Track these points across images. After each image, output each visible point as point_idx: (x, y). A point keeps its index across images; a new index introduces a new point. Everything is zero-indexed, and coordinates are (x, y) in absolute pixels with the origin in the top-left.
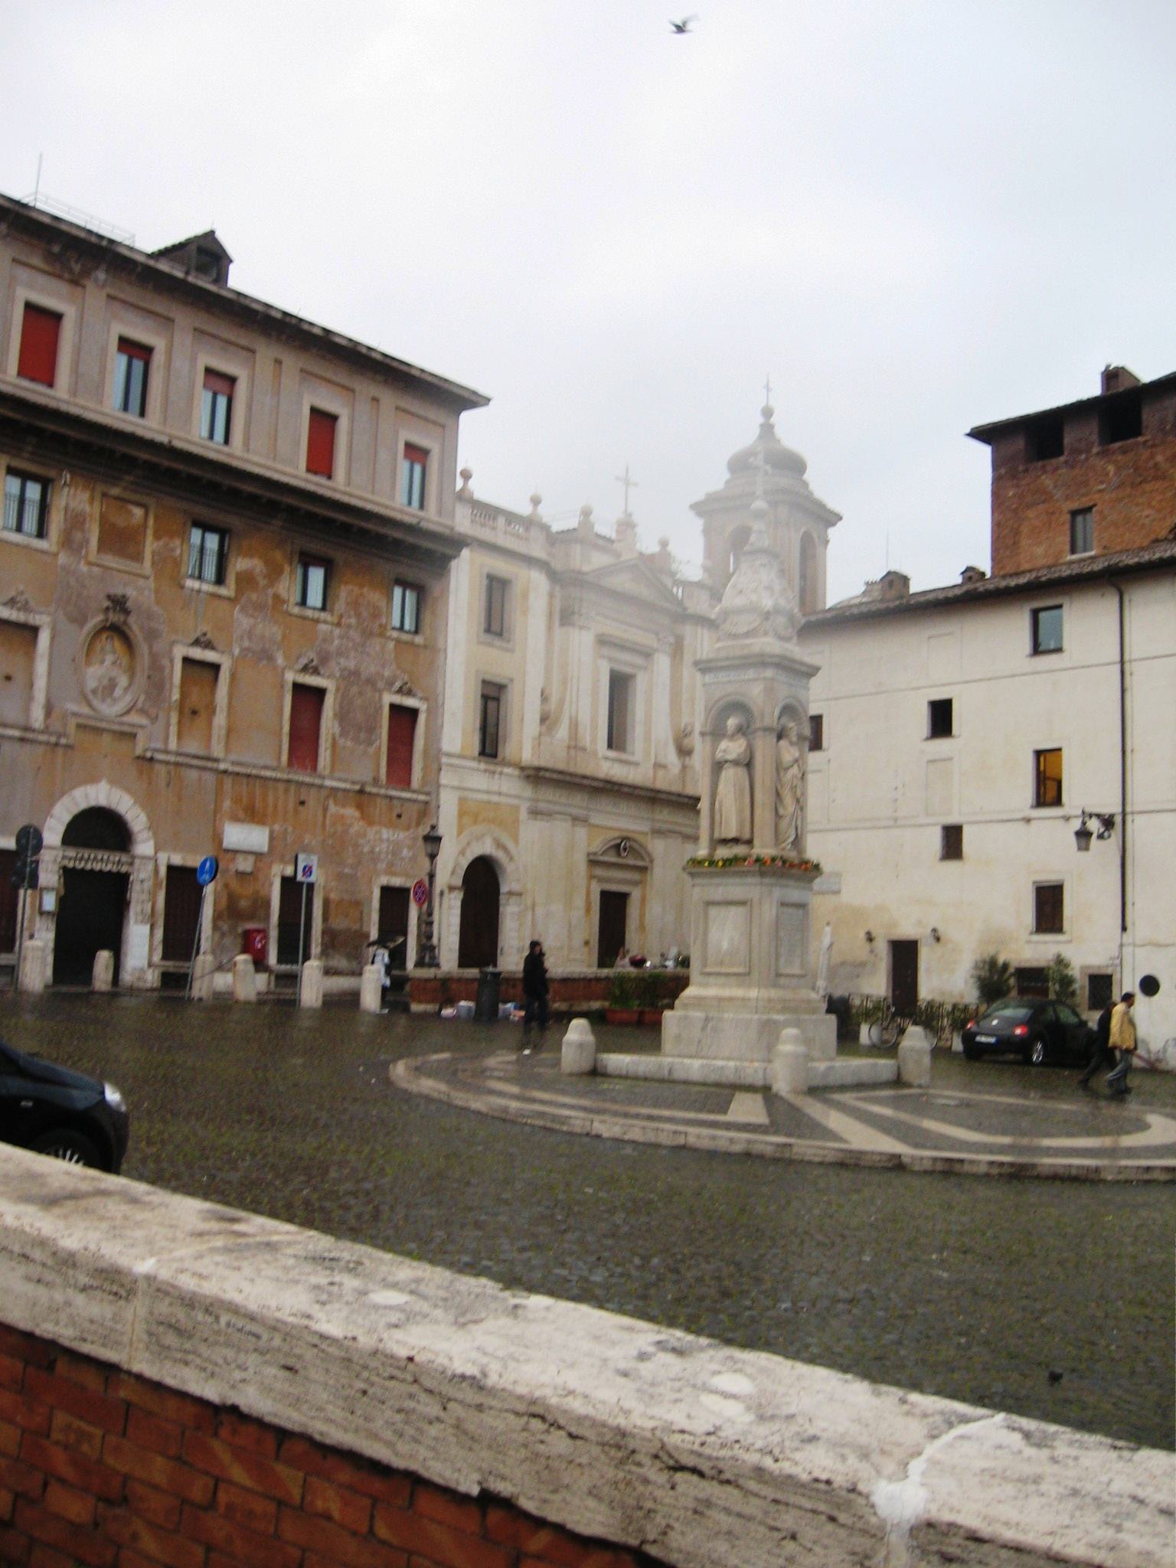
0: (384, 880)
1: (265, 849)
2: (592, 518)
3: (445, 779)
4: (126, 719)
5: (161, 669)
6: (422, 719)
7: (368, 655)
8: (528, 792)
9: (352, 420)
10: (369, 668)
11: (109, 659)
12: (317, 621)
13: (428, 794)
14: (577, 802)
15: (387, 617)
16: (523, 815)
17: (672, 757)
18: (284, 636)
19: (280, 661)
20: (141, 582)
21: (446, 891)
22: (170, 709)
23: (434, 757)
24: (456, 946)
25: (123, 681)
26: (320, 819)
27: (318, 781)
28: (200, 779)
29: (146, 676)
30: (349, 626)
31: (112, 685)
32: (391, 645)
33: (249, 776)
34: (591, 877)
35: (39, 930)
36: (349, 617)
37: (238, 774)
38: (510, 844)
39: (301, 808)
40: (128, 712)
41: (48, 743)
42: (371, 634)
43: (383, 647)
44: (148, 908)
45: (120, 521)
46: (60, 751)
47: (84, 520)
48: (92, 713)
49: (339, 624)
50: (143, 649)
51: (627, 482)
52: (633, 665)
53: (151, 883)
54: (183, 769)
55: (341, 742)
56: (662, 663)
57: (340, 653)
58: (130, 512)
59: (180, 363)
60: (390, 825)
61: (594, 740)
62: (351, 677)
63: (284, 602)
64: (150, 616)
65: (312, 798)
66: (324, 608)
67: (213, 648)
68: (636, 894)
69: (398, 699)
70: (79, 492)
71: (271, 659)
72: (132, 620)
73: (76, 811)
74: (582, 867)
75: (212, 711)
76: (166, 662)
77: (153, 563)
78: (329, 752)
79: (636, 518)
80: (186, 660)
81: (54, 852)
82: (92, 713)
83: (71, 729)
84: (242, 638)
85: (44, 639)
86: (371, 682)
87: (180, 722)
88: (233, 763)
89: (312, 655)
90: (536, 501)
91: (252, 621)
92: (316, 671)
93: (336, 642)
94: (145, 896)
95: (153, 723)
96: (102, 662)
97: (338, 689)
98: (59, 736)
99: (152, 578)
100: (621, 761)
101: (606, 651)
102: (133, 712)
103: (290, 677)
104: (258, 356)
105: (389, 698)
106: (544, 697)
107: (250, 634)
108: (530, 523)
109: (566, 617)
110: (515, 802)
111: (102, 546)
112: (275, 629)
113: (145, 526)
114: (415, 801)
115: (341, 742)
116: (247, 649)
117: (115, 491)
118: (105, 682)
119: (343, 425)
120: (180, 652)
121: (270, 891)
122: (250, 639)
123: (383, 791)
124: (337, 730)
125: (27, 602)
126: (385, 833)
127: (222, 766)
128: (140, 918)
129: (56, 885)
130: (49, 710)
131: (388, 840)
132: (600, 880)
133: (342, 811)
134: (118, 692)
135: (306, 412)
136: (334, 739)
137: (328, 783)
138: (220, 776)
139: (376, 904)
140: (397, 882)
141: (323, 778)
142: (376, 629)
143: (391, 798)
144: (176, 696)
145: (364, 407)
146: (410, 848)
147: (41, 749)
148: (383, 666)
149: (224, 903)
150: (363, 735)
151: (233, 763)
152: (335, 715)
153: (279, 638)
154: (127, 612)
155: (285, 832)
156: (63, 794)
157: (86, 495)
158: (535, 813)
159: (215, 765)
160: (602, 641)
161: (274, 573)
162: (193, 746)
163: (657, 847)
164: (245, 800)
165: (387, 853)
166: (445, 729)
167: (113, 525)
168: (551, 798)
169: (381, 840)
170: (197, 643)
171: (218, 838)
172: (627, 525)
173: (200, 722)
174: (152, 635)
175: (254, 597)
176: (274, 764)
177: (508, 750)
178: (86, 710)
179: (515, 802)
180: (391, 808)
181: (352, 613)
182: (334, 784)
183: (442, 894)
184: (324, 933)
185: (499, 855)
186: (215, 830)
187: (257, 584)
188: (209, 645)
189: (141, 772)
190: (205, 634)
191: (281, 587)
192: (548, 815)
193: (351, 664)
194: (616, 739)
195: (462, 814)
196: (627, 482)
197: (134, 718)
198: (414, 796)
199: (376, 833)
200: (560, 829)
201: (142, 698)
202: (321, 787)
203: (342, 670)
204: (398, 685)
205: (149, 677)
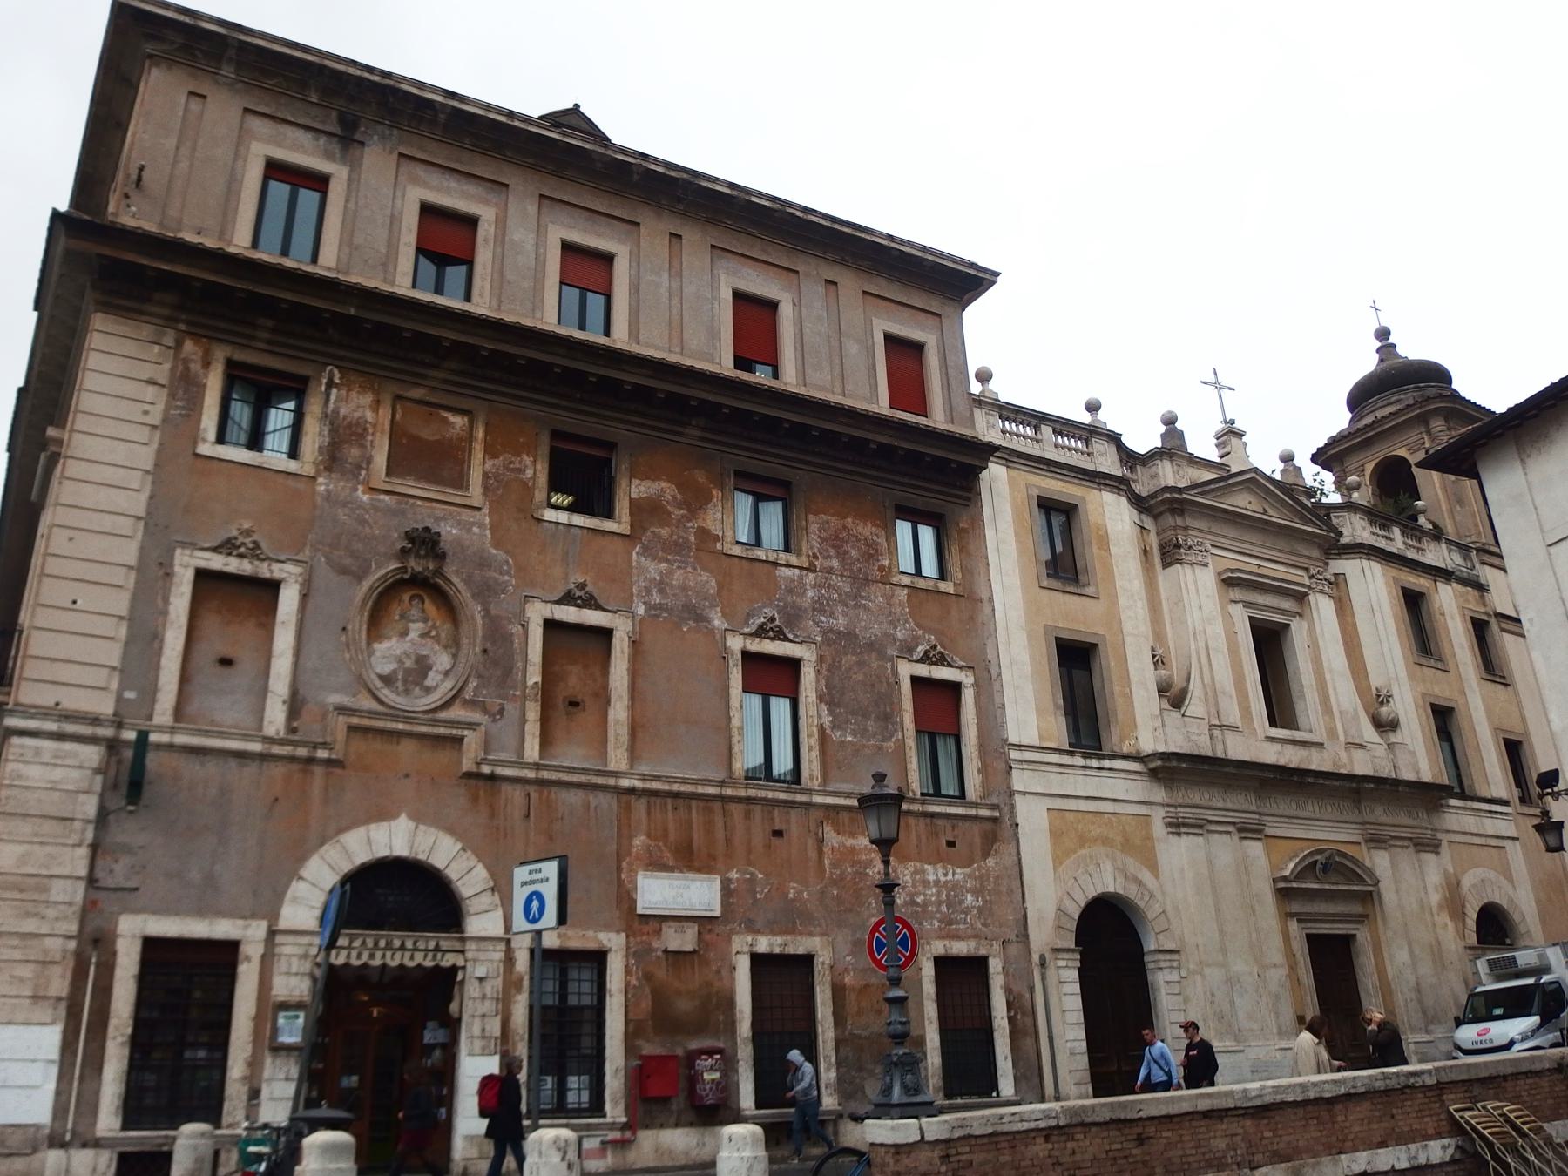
0: (939, 947)
1: (718, 913)
2: (1178, 425)
3: (1020, 780)
4: (443, 715)
5: (507, 638)
6: (968, 696)
7: (867, 609)
8: (1159, 794)
9: (798, 305)
10: (871, 627)
11: (416, 629)
12: (776, 564)
13: (994, 807)
14: (1239, 804)
15: (890, 553)
16: (1159, 829)
17: (1369, 733)
18: (720, 586)
19: (718, 622)
20: (466, 515)
22: (524, 697)
23: (997, 751)
24: (1083, 1046)
25: (443, 661)
26: (813, 854)
27: (804, 798)
28: (587, 806)
29: (477, 650)
30: (830, 571)
31: (423, 666)
32: (903, 594)
33: (677, 795)
35: (270, 1080)
36: (828, 557)
37: (655, 793)
38: (1146, 876)
39: (775, 841)
40: (446, 705)
41: (293, 759)
42: (867, 581)
43: (889, 598)
44: (495, 1027)
45: (428, 433)
46: (319, 771)
47: (365, 429)
48: (375, 706)
49: (811, 569)
50: (474, 611)
51: (1218, 386)
52: (1283, 611)
53: (499, 982)
54: (554, 789)
55: (836, 736)
56: (1323, 607)
57: (819, 608)
58: (445, 420)
59: (522, 235)
60: (937, 859)
61: (1246, 711)
62: (837, 643)
63: (717, 538)
64: (484, 563)
65: (794, 823)
66: (787, 549)
67: (598, 607)
68: (1363, 935)
69: (923, 670)
70: (354, 394)
71: (701, 619)
72: (450, 570)
73: (346, 867)
74: (1269, 897)
75: (603, 697)
76: (515, 629)
77: (487, 489)
78: (815, 753)
79: (1238, 425)
80: (550, 625)
81: (305, 940)
82: (375, 706)
83: (341, 735)
84: (648, 590)
85: (288, 599)
86: (875, 646)
87: (545, 721)
88: (644, 778)
89: (769, 612)
90: (1093, 407)
91: (664, 566)
92: (780, 635)
93: (810, 593)
94: (488, 1007)
95: (494, 721)
96: (404, 633)
97: (821, 659)
98: (315, 746)
99: (486, 511)
100: (1294, 742)
101: (1237, 594)
102: (457, 703)
103: (736, 643)
104: (642, 229)
105: (906, 670)
106: (1159, 662)
107: (662, 586)
108: (1089, 433)
109: (1170, 554)
110: (1142, 810)
111: (394, 467)
112: (705, 576)
113: (471, 438)
114: (976, 818)
115: (836, 736)
116: (659, 607)
117: (417, 393)
118: (409, 664)
119: (786, 312)
120: (537, 613)
121: (733, 980)
122: (661, 591)
124: (827, 720)
125: (257, 545)
126: (932, 873)
127: (625, 783)
128: (478, 1044)
129: (307, 999)
130: (295, 706)
131: (937, 882)
132: (1302, 918)
133: (850, 842)
134: (432, 678)
135: (727, 295)
136: (821, 728)
137: (818, 799)
138: (624, 798)
139: (929, 987)
140: (961, 948)
141: (810, 792)
143: (933, 815)
144: (534, 677)
145: (814, 292)
146: (977, 892)
147: (278, 770)
148: (894, 625)
149: (646, 1004)
150: (871, 725)
151: (644, 778)
152: (820, 698)
153: (712, 589)
154: (441, 557)
155: (753, 880)
156: (323, 841)
157: (368, 399)
158: (1176, 826)
159: (612, 781)
160: (1229, 582)
161: (696, 501)
162: (573, 755)
163: (1380, 862)
164: (672, 837)
165: (940, 903)
166: (1009, 710)
167: (415, 439)
168: (1197, 800)
169: (926, 883)
170: (567, 599)
171: (626, 898)
172: (1230, 434)
173: (587, 717)
174: (486, 592)
175: (665, 532)
176: (720, 776)
177: (1114, 738)
178: (369, 704)
179: (1142, 810)
180: (934, 834)
181: (832, 552)
182: (830, 800)
183: (1043, 965)
184: (838, 1043)
185: (1131, 892)
186: (620, 882)
187: (669, 514)
188: (590, 602)
189: (475, 799)
190: (582, 586)
191: (709, 517)
192: (1198, 827)
193: (840, 623)
194: (1280, 708)
195: (1056, 835)
196: (1218, 386)
197: (457, 713)
198: (973, 812)
199: (916, 872)
200: (1224, 848)
201: (473, 683)
202: (808, 806)
203: (824, 632)
204: (921, 649)
205: (485, 651)
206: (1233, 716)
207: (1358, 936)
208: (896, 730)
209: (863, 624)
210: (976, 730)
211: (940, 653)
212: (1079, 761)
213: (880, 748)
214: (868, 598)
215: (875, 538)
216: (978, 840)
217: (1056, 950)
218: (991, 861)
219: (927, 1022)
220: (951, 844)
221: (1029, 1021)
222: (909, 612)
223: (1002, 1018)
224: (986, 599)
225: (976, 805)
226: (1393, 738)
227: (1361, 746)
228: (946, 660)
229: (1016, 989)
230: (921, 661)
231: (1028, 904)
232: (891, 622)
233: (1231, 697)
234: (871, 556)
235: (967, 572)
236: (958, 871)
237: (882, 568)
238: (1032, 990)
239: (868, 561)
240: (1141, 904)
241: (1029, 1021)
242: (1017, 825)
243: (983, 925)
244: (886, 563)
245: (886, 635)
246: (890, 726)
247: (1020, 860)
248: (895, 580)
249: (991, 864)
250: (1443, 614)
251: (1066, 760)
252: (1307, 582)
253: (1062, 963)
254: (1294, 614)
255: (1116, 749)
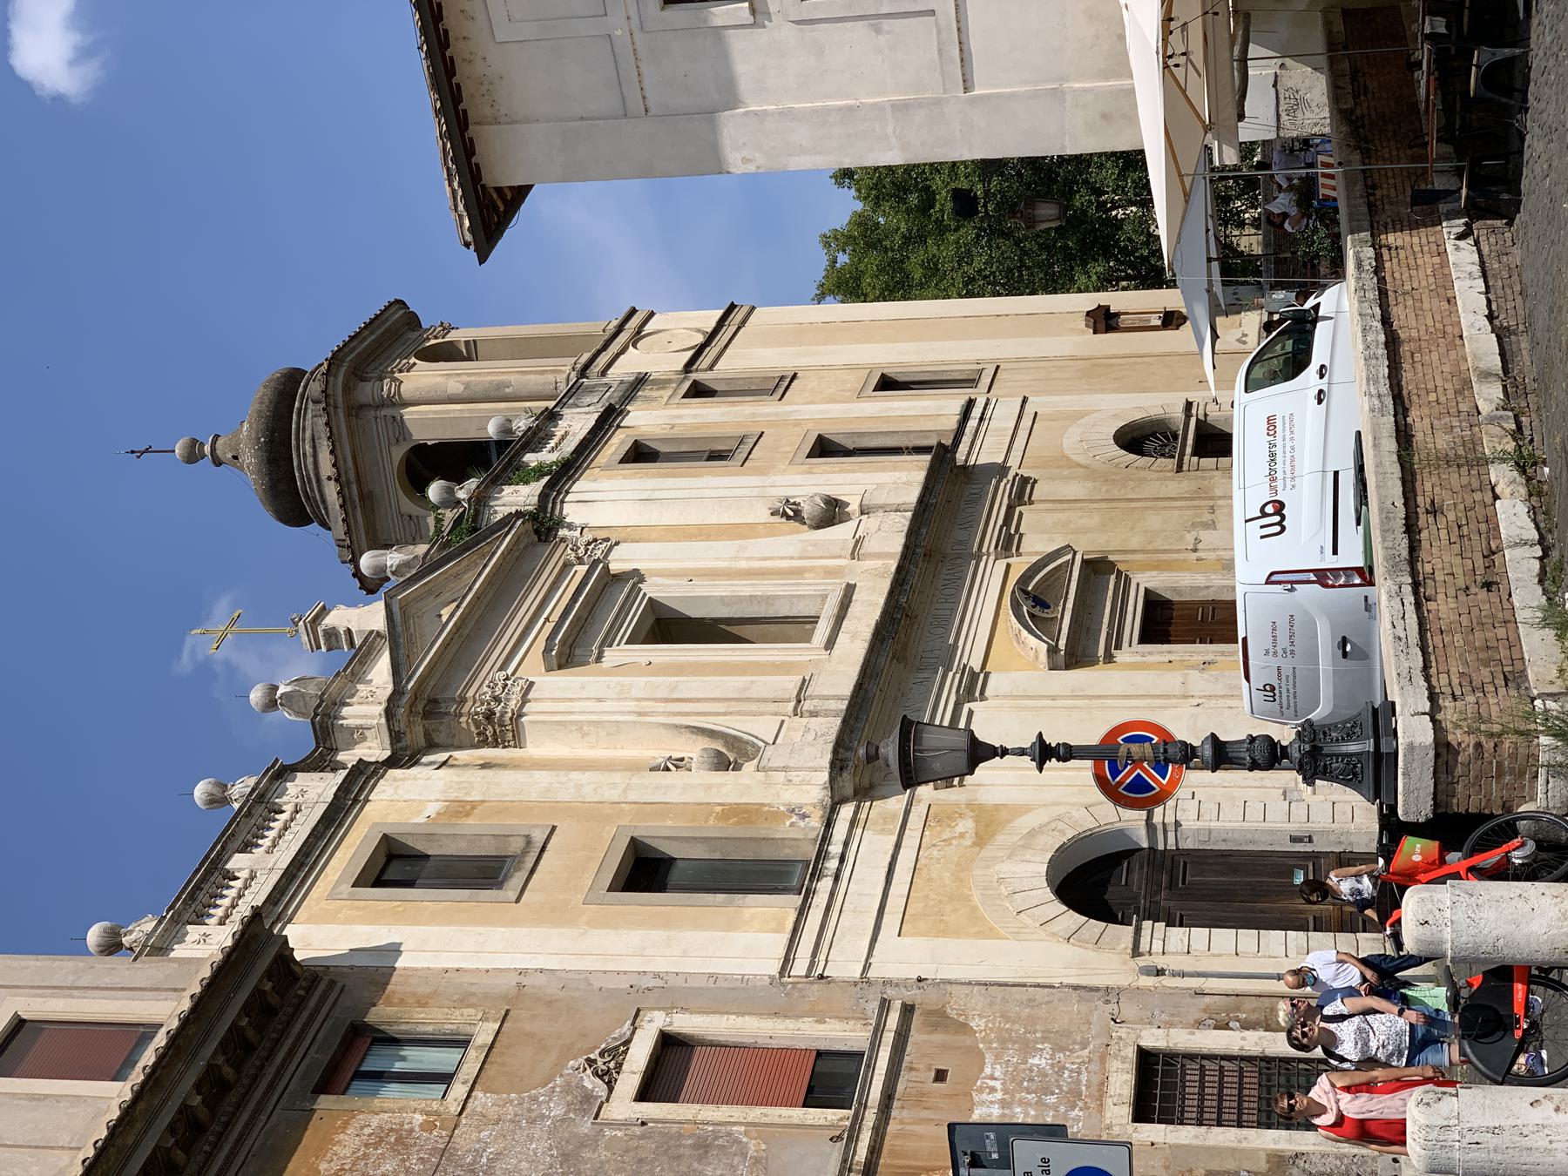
13: (885, 1005)
17: (840, 533)
21: (1142, 961)
34: (1109, 658)
38: (1026, 823)
105: (623, 1105)
123: (870, 1118)
131: (1003, 1104)
142: (438, 1136)
146: (1027, 1049)
165: (1040, 1103)
185: (1050, 844)
198: (889, 1038)
204: (590, 1082)
206: (790, 684)
207: (1149, 585)
208: (729, 1134)
209: (524, 1165)
210: (747, 1018)
211: (602, 1054)
212: (825, 885)
213: (757, 1161)
214: (478, 1154)
215: (367, 1131)
216: (938, 1038)
217: (1136, 952)
218: (976, 1023)
219: (1244, 1145)
220: (940, 1076)
221: (1250, 1004)
222: (518, 1093)
223: (1243, 1039)
224: (521, 979)
225: (878, 1031)
226: (853, 507)
227: (858, 543)
228: (617, 1047)
229: (1197, 1015)
230: (610, 1086)
231: (1056, 981)
232: (532, 1122)
233: (752, 682)
234: (399, 1140)
235: (464, 1000)
236: (988, 1071)
237: (428, 1127)
238: (1200, 993)
239: (406, 1146)
240: (1070, 834)
241: (1250, 1004)
242: (920, 980)
243: (1084, 1046)
244: (419, 1118)
245: (551, 1132)
246: (720, 1142)
247: (979, 984)
248: (454, 1108)
249: (982, 1023)
250: (673, 427)
251: (820, 900)
252: (582, 569)
253: (1157, 946)
254: (635, 590)
255: (813, 835)
